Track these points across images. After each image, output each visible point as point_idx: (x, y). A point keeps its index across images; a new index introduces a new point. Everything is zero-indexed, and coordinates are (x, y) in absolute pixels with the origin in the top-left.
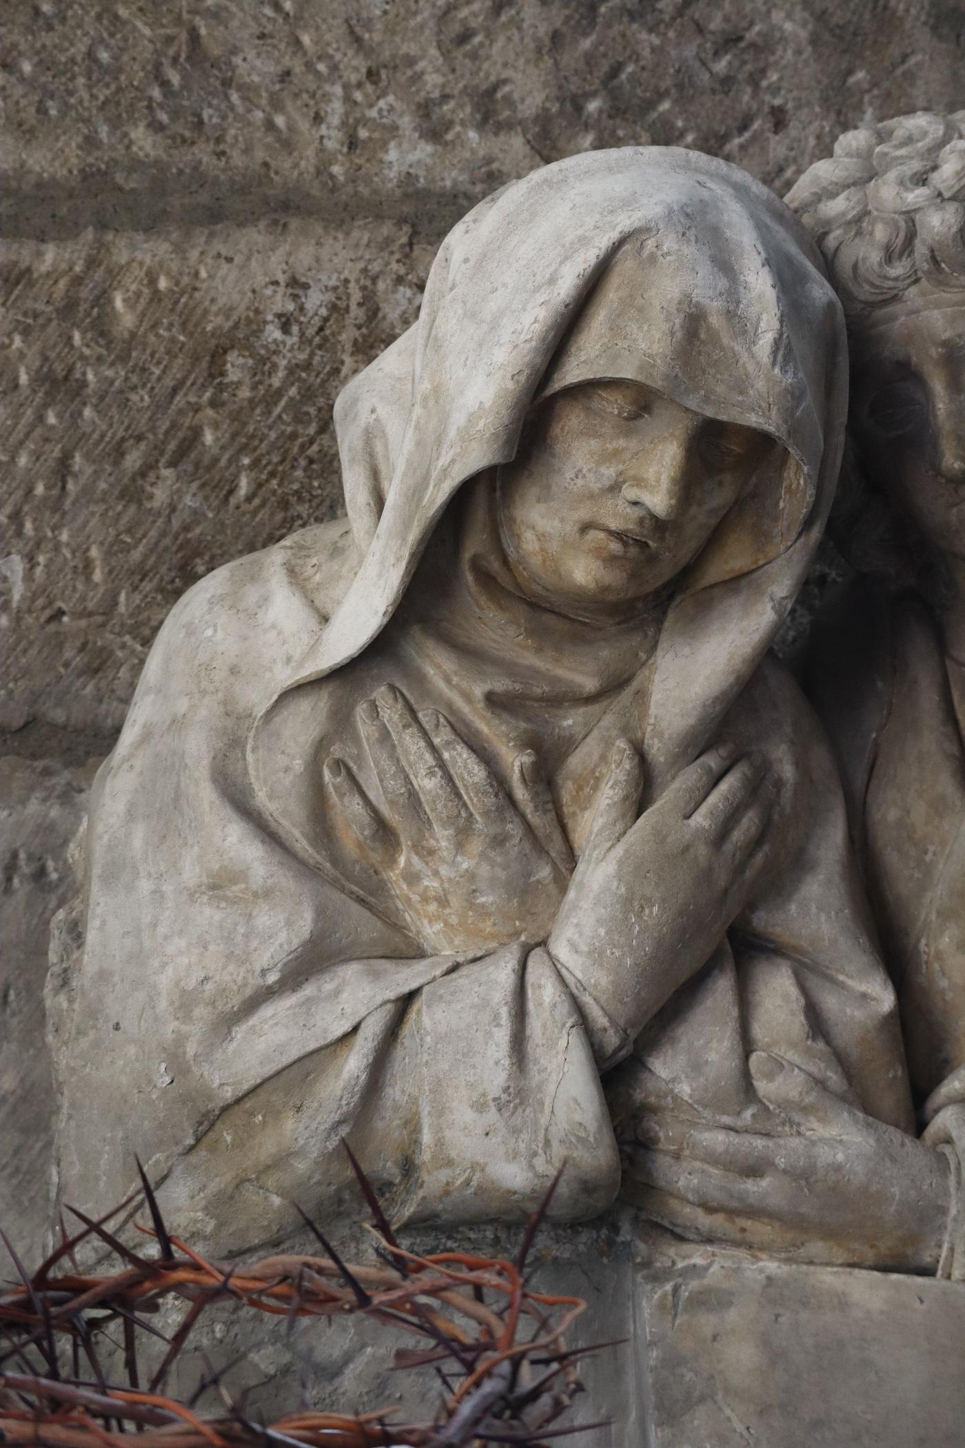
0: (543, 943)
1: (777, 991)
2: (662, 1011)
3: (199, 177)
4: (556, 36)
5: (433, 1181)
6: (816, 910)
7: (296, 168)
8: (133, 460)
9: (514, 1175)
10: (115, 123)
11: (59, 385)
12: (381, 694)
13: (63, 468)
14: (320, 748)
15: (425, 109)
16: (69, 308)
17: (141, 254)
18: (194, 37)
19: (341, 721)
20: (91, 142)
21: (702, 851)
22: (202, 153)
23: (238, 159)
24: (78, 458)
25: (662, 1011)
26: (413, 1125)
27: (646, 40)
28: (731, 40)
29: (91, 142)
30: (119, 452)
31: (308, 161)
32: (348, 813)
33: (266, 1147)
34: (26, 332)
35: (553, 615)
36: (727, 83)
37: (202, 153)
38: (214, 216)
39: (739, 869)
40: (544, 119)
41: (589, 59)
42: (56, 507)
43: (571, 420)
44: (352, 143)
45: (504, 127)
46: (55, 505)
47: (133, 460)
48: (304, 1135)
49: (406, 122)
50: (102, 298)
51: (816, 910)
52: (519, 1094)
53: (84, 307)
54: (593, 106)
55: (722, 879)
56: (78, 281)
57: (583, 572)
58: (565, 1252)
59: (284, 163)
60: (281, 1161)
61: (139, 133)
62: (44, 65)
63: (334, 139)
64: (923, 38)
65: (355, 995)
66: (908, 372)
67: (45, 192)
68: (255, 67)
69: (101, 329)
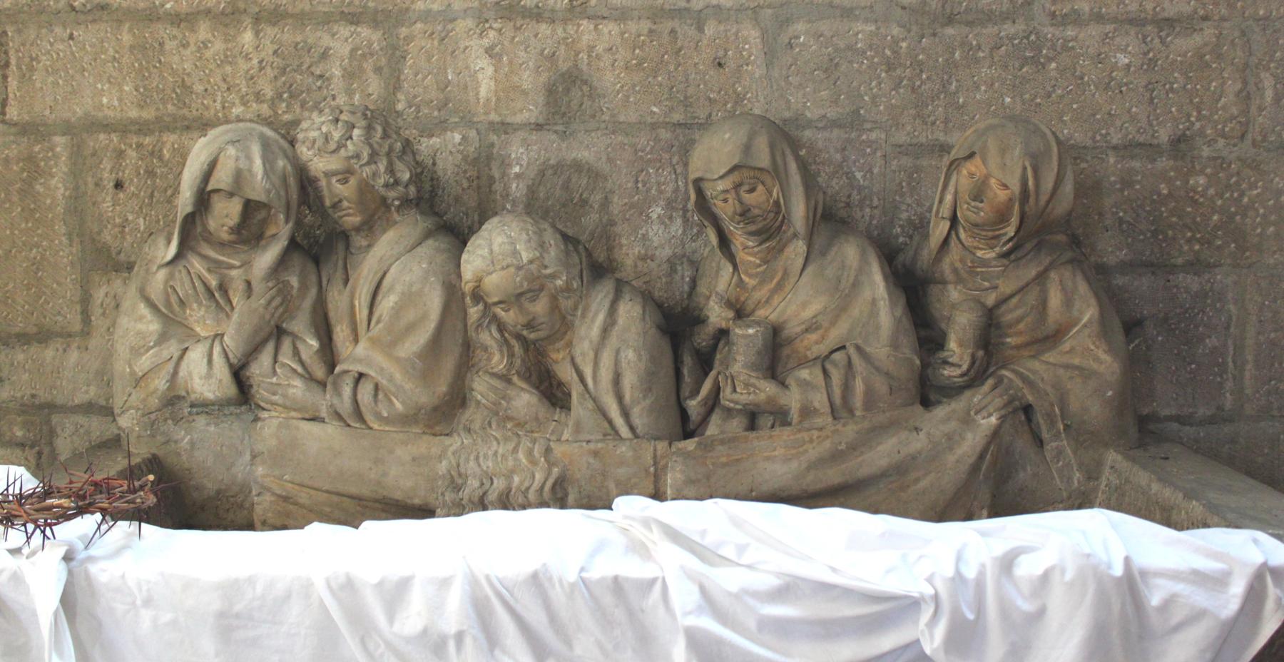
0: (223, 335)
1: (287, 345)
2: (253, 351)
3: (184, 118)
4: (275, 77)
5: (193, 397)
6: (300, 325)
7: (209, 114)
8: (169, 192)
9: (210, 396)
10: (164, 104)
11: (151, 173)
12: (181, 268)
13: (152, 196)
14: (166, 282)
15: (242, 97)
16: (152, 154)
17: (170, 139)
18: (183, 80)
19: (171, 276)
20: (158, 109)
21: (261, 309)
22: (185, 111)
24: (156, 194)
25: (253, 351)
26: (186, 382)
28: (321, 76)
29: (158, 109)
30: (166, 191)
31: (212, 112)
32: (173, 299)
33: (152, 387)
35: (221, 245)
36: (320, 88)
37: (185, 111)
39: (273, 315)
40: (272, 99)
41: (284, 83)
42: (150, 204)
43: (215, 198)
44: (224, 108)
45: (262, 102)
46: (150, 204)
47: (169, 192)
48: (160, 383)
49: (237, 101)
50: (161, 150)
51: (300, 325)
52: (209, 375)
53: (156, 153)
54: (285, 96)
55: (267, 317)
57: (225, 236)
59: (206, 113)
60: (156, 390)
61: (169, 106)
62: (145, 89)
63: (218, 105)
64: (371, 74)
65: (172, 348)
66: (316, 180)
67: (147, 122)
68: (199, 88)
69: (160, 158)
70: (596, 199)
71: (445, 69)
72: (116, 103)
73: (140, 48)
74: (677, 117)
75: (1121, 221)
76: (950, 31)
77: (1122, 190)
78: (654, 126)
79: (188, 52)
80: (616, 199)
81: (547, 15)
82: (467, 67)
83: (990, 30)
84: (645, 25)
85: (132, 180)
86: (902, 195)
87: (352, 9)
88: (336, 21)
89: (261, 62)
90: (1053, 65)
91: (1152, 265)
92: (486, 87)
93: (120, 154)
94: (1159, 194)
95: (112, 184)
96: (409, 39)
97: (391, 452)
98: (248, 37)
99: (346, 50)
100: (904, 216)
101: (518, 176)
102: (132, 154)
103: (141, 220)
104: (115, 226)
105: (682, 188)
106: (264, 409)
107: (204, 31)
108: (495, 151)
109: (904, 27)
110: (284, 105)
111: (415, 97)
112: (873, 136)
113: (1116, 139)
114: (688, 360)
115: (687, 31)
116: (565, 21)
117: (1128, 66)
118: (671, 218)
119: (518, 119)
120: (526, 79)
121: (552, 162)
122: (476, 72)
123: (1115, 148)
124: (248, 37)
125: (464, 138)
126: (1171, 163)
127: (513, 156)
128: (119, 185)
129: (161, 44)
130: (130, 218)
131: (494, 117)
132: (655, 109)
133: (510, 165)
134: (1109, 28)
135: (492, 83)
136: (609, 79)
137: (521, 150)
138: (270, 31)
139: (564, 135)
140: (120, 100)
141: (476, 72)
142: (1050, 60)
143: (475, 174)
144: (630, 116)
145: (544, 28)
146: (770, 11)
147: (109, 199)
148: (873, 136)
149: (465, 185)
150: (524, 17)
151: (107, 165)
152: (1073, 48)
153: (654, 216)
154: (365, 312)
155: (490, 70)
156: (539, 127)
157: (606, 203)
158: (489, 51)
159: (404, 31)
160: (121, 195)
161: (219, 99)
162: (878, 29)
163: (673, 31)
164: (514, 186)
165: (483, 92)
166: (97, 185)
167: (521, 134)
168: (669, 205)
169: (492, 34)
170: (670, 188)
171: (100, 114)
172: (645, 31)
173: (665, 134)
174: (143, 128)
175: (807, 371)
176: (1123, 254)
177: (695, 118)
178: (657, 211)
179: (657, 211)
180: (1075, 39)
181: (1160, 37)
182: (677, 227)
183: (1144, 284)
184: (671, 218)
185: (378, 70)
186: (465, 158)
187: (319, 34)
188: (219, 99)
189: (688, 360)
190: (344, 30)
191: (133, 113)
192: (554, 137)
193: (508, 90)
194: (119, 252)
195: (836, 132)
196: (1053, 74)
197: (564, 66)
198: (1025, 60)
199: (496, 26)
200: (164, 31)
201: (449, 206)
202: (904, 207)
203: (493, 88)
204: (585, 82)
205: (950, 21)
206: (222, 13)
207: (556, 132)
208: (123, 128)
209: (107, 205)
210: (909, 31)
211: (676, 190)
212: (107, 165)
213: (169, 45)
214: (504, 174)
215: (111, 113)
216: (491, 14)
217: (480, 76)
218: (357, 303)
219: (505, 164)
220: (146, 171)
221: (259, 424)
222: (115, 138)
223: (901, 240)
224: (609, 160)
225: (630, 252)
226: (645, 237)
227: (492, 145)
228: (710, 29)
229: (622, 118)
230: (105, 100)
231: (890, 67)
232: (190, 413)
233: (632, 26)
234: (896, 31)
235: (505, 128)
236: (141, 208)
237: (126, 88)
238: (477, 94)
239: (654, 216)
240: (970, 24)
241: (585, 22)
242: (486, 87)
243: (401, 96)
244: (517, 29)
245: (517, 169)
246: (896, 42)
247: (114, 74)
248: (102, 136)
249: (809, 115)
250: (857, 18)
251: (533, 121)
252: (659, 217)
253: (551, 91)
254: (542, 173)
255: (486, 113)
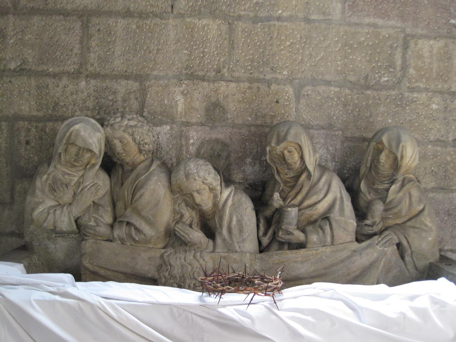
8: (48, 146)
11: (41, 138)
13: (41, 147)
16: (42, 130)
17: (50, 124)
23: (60, 113)
24: (43, 146)
27: (103, 101)
34: (37, 132)
38: (57, 120)
44: (72, 112)
45: (88, 110)
49: (78, 110)
50: (45, 129)
53: (43, 130)
56: (43, 127)
58: (75, 236)
62: (40, 103)
63: (70, 111)
68: (62, 104)
69: (45, 132)
70: (224, 154)
71: (164, 99)
72: (28, 109)
73: (38, 87)
74: (259, 122)
75: (432, 171)
76: (369, 92)
77: (433, 159)
78: (250, 126)
79: (58, 89)
80: (232, 155)
81: (207, 78)
82: (174, 99)
83: (384, 93)
84: (247, 84)
85: (33, 140)
86: (348, 157)
87: (127, 74)
88: (120, 78)
89: (88, 94)
90: (408, 108)
91: (444, 189)
92: (181, 107)
93: (29, 130)
94: (447, 161)
95: (24, 142)
96: (149, 87)
97: (139, 255)
98: (83, 83)
99: (123, 91)
100: (348, 166)
101: (193, 144)
102: (34, 130)
103: (36, 158)
104: (25, 159)
105: (260, 151)
106: (87, 236)
107: (65, 81)
108: (183, 133)
109: (350, 90)
110: (97, 112)
111: (151, 110)
112: (337, 133)
113: (432, 138)
114: (262, 221)
115: (263, 87)
116: (214, 81)
117: (437, 109)
118: (255, 163)
119: (194, 120)
120: (197, 104)
121: (207, 139)
122: (177, 101)
123: (431, 142)
124: (83, 83)
125: (172, 128)
126: (453, 149)
127: (191, 136)
128: (28, 143)
129: (48, 86)
130: (32, 156)
131: (183, 119)
132: (250, 119)
133: (190, 140)
134: (430, 94)
135: (183, 106)
136: (232, 106)
137: (194, 133)
138: (93, 82)
139: (212, 128)
140: (29, 108)
141: (177, 101)
142: (407, 105)
143: (175, 143)
144: (240, 121)
145: (205, 84)
146: (297, 81)
147: (23, 148)
148: (337, 133)
149: (171, 146)
150: (197, 79)
151: (23, 134)
152: (416, 101)
153: (248, 162)
154: (131, 197)
155: (182, 100)
156: (202, 124)
157: (228, 157)
158: (182, 93)
159: (148, 84)
160: (29, 147)
161: (70, 108)
162: (340, 90)
163: (258, 88)
164: (191, 148)
165: (179, 109)
166: (19, 142)
167: (195, 127)
168: (254, 159)
169: (184, 85)
170: (255, 151)
171: (21, 114)
172: (246, 87)
173: (253, 129)
174: (38, 120)
175: (312, 226)
176: (433, 184)
177: (265, 123)
178: (248, 160)
179: (248, 160)
180: (416, 98)
181: (450, 99)
182: (257, 167)
183: (440, 196)
184: (255, 163)
185: (136, 99)
186: (171, 136)
187: (113, 83)
188: (70, 108)
189: (262, 221)
190: (123, 82)
191: (35, 113)
192: (208, 128)
193: (189, 109)
194: (26, 170)
195: (322, 131)
196: (408, 111)
197: (213, 100)
198: (398, 106)
199: (186, 82)
200: (50, 81)
201: (164, 155)
202: (348, 162)
203: (184, 108)
204: (221, 107)
205: (368, 88)
206: (73, 73)
207: (209, 126)
208: (29, 119)
209: (22, 150)
210: (352, 92)
211: (257, 152)
212: (23, 134)
213: (51, 86)
214: (187, 144)
215: (25, 113)
216: (183, 77)
217: (179, 102)
218: (126, 193)
219: (187, 139)
220: (39, 137)
221: (84, 242)
222: (26, 123)
223: (347, 175)
224: (231, 139)
225: (238, 176)
226: (244, 171)
227: (182, 131)
228: (274, 87)
229: (236, 122)
230: (23, 108)
231: (345, 106)
232: (55, 236)
233: (242, 85)
234: (347, 91)
235: (187, 124)
236: (36, 152)
237: (32, 103)
238: (177, 110)
239: (248, 162)
240: (375, 90)
241: (222, 82)
242: (181, 107)
243: (145, 110)
244: (194, 84)
245: (192, 141)
246: (346, 95)
247: (27, 97)
248: (21, 122)
249: (311, 123)
250: (331, 86)
251: (199, 121)
252: (250, 163)
253: (207, 110)
254: (202, 143)
255: (181, 118)
